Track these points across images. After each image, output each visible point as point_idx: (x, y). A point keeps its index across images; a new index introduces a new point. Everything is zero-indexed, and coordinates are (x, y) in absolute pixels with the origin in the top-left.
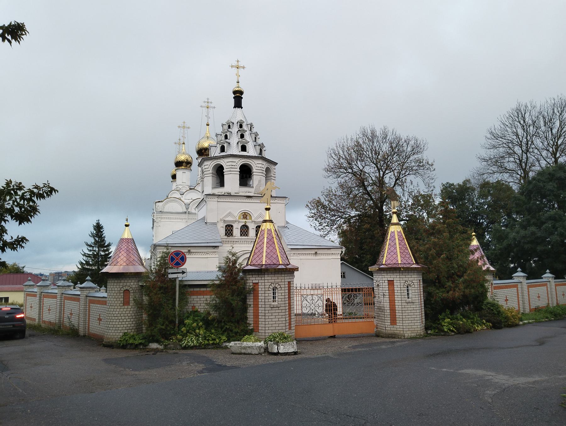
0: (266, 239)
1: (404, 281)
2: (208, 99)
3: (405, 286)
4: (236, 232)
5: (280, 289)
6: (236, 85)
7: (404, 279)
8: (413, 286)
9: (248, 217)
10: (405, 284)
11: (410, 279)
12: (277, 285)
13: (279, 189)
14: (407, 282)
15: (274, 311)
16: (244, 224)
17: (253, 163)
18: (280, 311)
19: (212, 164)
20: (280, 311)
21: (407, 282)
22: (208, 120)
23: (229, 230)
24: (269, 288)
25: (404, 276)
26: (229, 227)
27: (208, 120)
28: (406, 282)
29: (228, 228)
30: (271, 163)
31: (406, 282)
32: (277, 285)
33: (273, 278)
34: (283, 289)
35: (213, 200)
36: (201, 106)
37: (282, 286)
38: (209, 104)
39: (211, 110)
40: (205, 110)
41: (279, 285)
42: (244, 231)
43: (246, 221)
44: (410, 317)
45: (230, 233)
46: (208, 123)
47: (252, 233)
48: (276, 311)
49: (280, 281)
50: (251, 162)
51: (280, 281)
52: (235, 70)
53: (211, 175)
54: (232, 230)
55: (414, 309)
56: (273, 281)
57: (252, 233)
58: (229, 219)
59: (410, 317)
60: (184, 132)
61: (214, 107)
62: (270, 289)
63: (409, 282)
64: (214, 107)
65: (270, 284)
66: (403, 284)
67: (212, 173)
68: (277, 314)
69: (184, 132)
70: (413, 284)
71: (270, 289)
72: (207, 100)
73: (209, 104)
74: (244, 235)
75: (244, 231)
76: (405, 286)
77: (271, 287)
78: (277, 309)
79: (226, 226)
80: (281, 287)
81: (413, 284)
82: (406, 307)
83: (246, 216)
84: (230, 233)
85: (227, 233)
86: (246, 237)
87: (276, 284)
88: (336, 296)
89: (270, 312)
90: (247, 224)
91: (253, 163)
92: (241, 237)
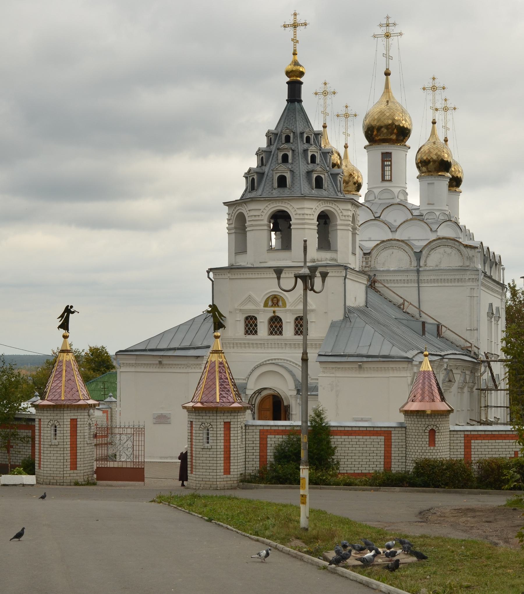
0: (64, 371)
1: (201, 423)
2: (388, 18)
3: (200, 429)
4: (263, 328)
5: (59, 426)
6: (291, 58)
7: (200, 420)
8: (212, 429)
9: (280, 303)
10: (201, 426)
11: (207, 421)
12: (56, 422)
13: (78, 312)
14: (203, 425)
15: (52, 449)
16: (272, 314)
17: (290, 208)
18: (58, 449)
19: (234, 212)
20: (58, 449)
21: (203, 425)
22: (388, 64)
23: (251, 325)
24: (48, 424)
25: (201, 417)
26: (251, 319)
27: (388, 64)
28: (202, 423)
29: (249, 322)
30: (335, 201)
31: (202, 423)
32: (56, 422)
33: (52, 415)
34: (61, 426)
35: (223, 277)
36: (375, 36)
37: (60, 423)
38: (391, 29)
39: (393, 40)
40: (382, 41)
41: (58, 422)
42: (276, 327)
43: (276, 309)
44: (205, 465)
45: (254, 329)
46: (387, 69)
47: (288, 329)
48: (55, 449)
49: (59, 417)
50: (288, 206)
51: (59, 417)
52: (290, 30)
53: (233, 231)
54: (256, 325)
55: (211, 456)
56: (52, 418)
57: (288, 329)
58: (250, 307)
59: (205, 465)
60: (325, 103)
61: (401, 34)
62: (48, 426)
63: (206, 424)
64: (401, 34)
65: (49, 420)
66: (199, 426)
67: (235, 228)
68: (56, 452)
69: (325, 103)
70: (211, 426)
71: (48, 426)
72: (384, 22)
73: (391, 29)
74: (276, 333)
75: (276, 327)
76: (200, 429)
77: (49, 423)
78: (56, 447)
79: (247, 318)
80: (59, 424)
81: (211, 426)
82: (201, 453)
83: (278, 301)
84: (254, 329)
85: (249, 329)
86: (279, 337)
87: (55, 421)
88: (138, 437)
89: (48, 449)
90: (277, 314)
91: (290, 208)
92: (272, 337)
